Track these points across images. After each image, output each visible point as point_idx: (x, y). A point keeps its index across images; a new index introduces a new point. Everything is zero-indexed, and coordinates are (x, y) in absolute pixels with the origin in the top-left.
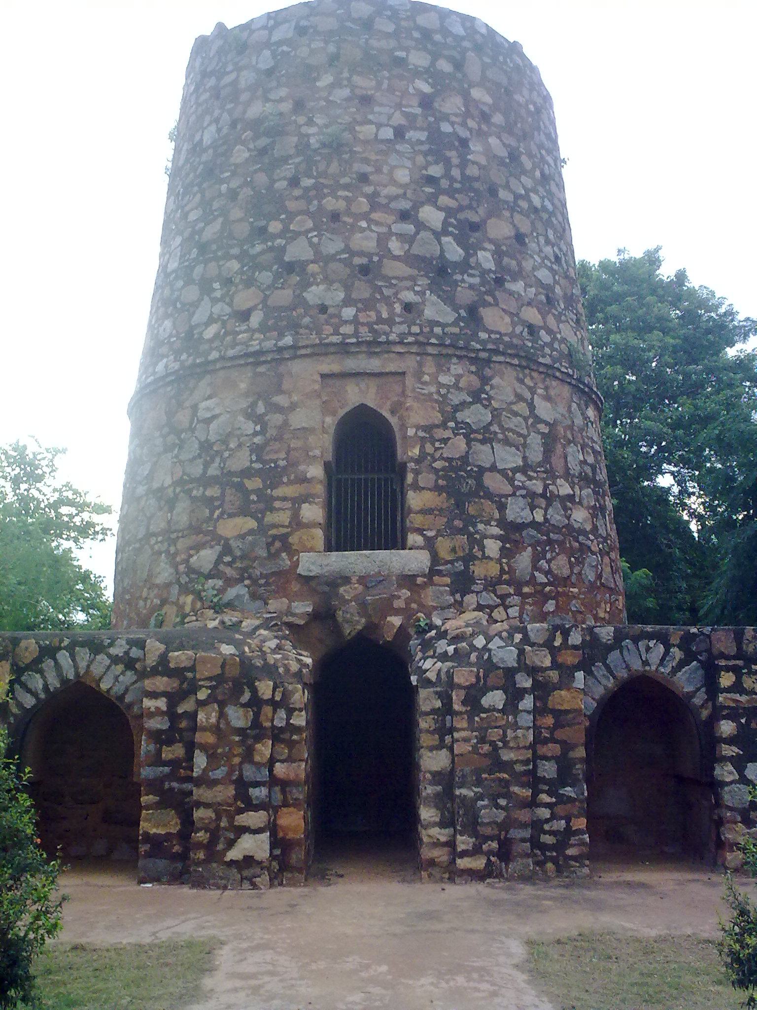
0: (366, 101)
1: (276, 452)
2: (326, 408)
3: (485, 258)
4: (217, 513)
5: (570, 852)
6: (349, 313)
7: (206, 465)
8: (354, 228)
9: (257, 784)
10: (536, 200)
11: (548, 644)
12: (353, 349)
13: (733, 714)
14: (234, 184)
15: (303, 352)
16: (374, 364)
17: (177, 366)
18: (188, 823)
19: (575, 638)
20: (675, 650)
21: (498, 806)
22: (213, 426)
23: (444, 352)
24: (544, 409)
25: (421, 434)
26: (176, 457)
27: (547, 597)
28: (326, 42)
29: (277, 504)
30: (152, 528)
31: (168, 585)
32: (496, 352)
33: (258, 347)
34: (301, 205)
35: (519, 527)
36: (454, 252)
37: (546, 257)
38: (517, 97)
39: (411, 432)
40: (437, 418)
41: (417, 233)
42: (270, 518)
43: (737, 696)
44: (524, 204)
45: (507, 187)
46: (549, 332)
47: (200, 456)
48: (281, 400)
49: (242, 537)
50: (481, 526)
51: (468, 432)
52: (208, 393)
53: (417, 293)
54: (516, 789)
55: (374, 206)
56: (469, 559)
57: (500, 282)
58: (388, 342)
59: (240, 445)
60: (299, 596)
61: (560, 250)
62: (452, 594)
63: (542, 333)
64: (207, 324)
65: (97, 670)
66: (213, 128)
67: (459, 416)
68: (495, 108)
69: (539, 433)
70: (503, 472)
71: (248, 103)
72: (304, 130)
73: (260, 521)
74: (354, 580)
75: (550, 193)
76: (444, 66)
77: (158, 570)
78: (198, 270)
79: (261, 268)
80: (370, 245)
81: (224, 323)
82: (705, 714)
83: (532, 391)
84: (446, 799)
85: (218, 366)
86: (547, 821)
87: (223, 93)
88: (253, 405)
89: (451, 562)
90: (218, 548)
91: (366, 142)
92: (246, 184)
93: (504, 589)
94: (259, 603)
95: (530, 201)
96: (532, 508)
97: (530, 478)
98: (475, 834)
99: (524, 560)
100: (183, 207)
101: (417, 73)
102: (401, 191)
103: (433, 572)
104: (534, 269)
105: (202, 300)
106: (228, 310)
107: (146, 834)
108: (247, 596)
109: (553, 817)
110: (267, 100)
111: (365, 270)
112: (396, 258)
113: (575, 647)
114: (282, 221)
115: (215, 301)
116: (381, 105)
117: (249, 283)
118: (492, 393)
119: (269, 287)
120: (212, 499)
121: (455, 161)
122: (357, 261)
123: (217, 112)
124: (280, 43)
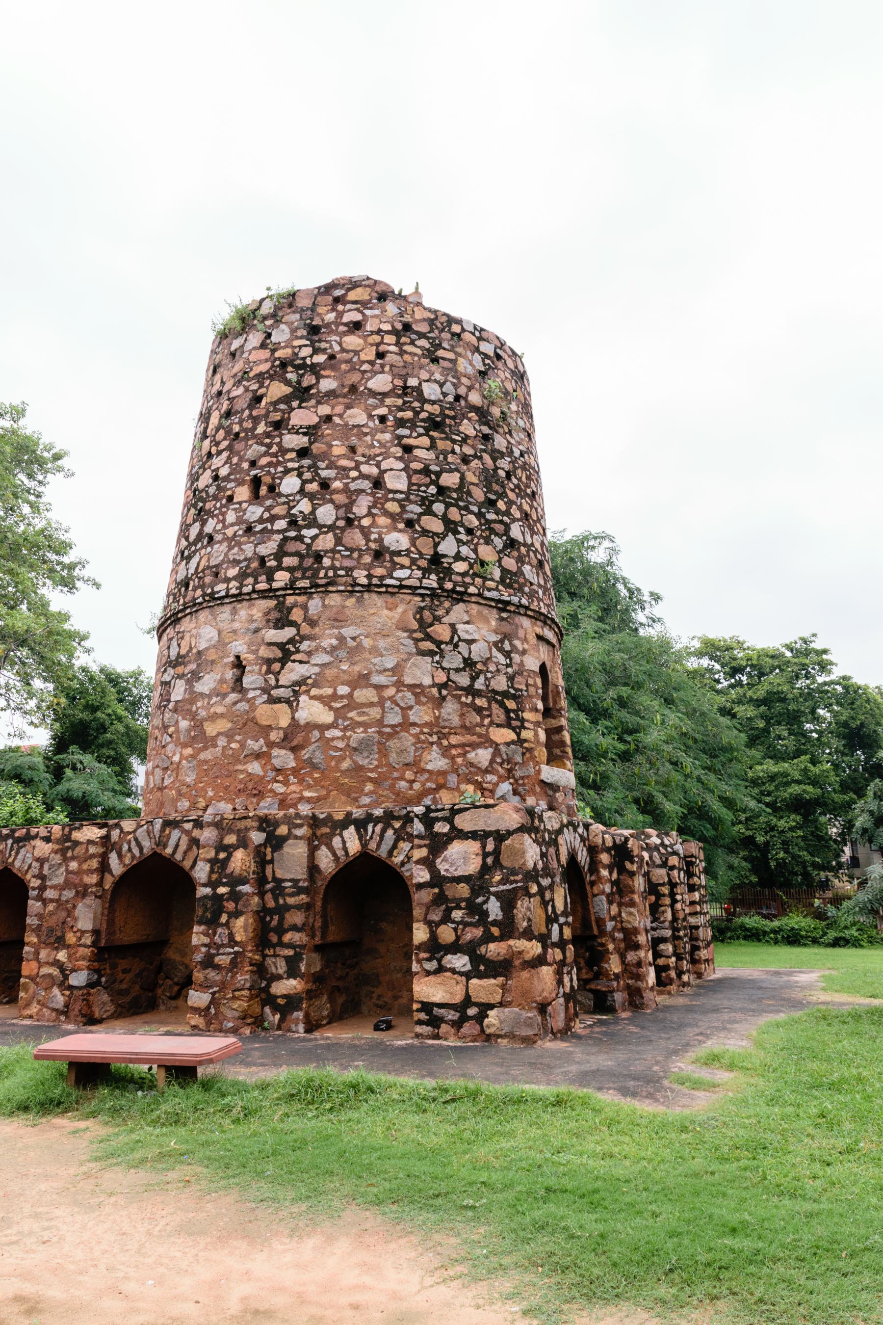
7: (473, 679)
14: (468, 450)
15: (529, 613)
26: (437, 662)
33: (508, 599)
49: (508, 744)
52: (466, 618)
59: (498, 670)
73: (518, 734)
77: (429, 758)
81: (471, 566)
85: (473, 599)
88: (502, 641)
90: (491, 750)
106: (474, 556)
114: (505, 503)
117: (488, 541)
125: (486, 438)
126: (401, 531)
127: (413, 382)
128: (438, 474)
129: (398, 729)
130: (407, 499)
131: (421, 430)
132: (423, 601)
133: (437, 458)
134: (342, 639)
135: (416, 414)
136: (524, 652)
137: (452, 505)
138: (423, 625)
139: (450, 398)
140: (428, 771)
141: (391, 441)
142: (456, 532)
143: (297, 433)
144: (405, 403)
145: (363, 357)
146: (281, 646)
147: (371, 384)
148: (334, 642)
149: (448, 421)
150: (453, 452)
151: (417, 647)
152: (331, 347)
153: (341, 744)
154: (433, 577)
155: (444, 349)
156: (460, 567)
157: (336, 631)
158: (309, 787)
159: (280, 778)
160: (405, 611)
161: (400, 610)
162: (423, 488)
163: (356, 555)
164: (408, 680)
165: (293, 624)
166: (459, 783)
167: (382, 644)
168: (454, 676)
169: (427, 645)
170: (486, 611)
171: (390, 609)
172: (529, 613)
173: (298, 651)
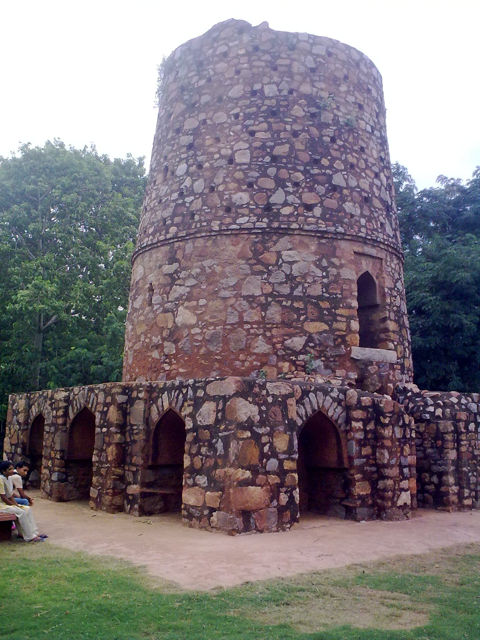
1: (336, 289)
4: (302, 318)
7: (292, 289)
8: (360, 177)
14: (296, 127)
15: (347, 237)
29: (339, 318)
33: (325, 229)
42: (335, 325)
48: (335, 260)
49: (320, 333)
52: (290, 246)
59: (315, 282)
74: (374, 363)
77: (256, 345)
80: (367, 187)
81: (296, 209)
88: (320, 260)
90: (305, 338)
92: (303, 130)
94: (329, 371)
105: (278, 189)
106: (299, 202)
107: (359, 495)
108: (323, 367)
114: (329, 160)
117: (311, 189)
119: (323, 196)
120: (298, 309)
124: (318, 56)
125: (313, 115)
126: (244, 191)
127: (257, 87)
128: (272, 148)
129: (236, 326)
130: (250, 169)
131: (261, 119)
132: (256, 238)
133: (272, 136)
134: (203, 268)
135: (259, 108)
136: (342, 266)
137: (283, 168)
138: (256, 253)
139: (285, 93)
140: (255, 354)
141: (242, 130)
142: (284, 186)
143: (187, 134)
144: (251, 102)
145: (227, 76)
146: (170, 275)
147: (230, 94)
148: (198, 270)
149: (281, 109)
150: (285, 130)
151: (251, 269)
152: (209, 73)
153: (200, 338)
154: (265, 220)
155: (282, 58)
156: (286, 211)
157: (200, 263)
158: (182, 367)
159: (167, 360)
160: (244, 246)
161: (241, 245)
162: (260, 159)
163: (213, 211)
164: (244, 293)
165: (177, 261)
166: (277, 361)
167: (228, 269)
168: (277, 288)
169: (259, 267)
170: (306, 240)
171: (234, 245)
172: (347, 237)
173: (179, 278)
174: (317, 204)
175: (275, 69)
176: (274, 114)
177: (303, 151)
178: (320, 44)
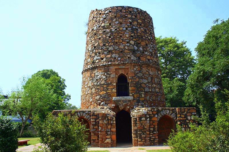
0: (121, 23)
2: (116, 74)
3: (141, 49)
5: (155, 141)
6: (119, 59)
7: (97, 83)
9: (109, 132)
10: (149, 38)
11: (151, 111)
12: (120, 65)
13: (180, 121)
14: (100, 37)
16: (124, 67)
17: (92, 67)
18: (98, 137)
19: (155, 110)
20: (171, 111)
21: (144, 135)
22: (98, 77)
23: (135, 65)
24: (151, 73)
25: (131, 78)
27: (152, 103)
28: (114, 14)
29: (109, 89)
30: (88, 93)
31: (92, 102)
32: (143, 64)
34: (111, 41)
35: (147, 92)
36: (136, 48)
37: (151, 47)
38: (146, 20)
39: (130, 78)
40: (134, 75)
41: (130, 45)
43: (180, 118)
44: (147, 39)
45: (144, 36)
46: (152, 60)
47: (96, 81)
50: (141, 92)
51: (139, 78)
53: (130, 55)
54: (147, 132)
55: (123, 41)
56: (139, 98)
57: (143, 52)
58: (126, 63)
59: (103, 80)
60: (113, 104)
61: (154, 45)
62: (137, 103)
63: (151, 60)
64: (96, 60)
65: (84, 115)
66: (96, 27)
67: (137, 75)
68: (142, 23)
69: (150, 77)
70: (144, 84)
71: (102, 24)
72: (111, 28)
75: (152, 36)
76: (133, 17)
78: (94, 51)
79: (105, 51)
82: (176, 121)
83: (149, 70)
84: (136, 134)
85: (99, 67)
86: (152, 137)
87: (97, 21)
89: (137, 98)
91: (121, 30)
92: (102, 37)
93: (145, 102)
95: (148, 38)
96: (149, 89)
97: (149, 84)
98: (141, 139)
99: (148, 98)
100: (91, 40)
101: (129, 18)
102: (127, 38)
103: (134, 100)
104: (149, 49)
107: (92, 139)
109: (153, 136)
110: (105, 23)
111: (122, 52)
112: (127, 50)
113: (155, 111)
115: (97, 56)
116: (124, 24)
118: (143, 71)
121: (136, 33)
122: (120, 50)
123: (96, 24)
124: (106, 14)
125: (104, 32)
136: (111, 74)
137: (97, 49)
174: (104, 58)
175: (96, 22)
176: (96, 34)
177: (101, 43)
178: (107, 10)
